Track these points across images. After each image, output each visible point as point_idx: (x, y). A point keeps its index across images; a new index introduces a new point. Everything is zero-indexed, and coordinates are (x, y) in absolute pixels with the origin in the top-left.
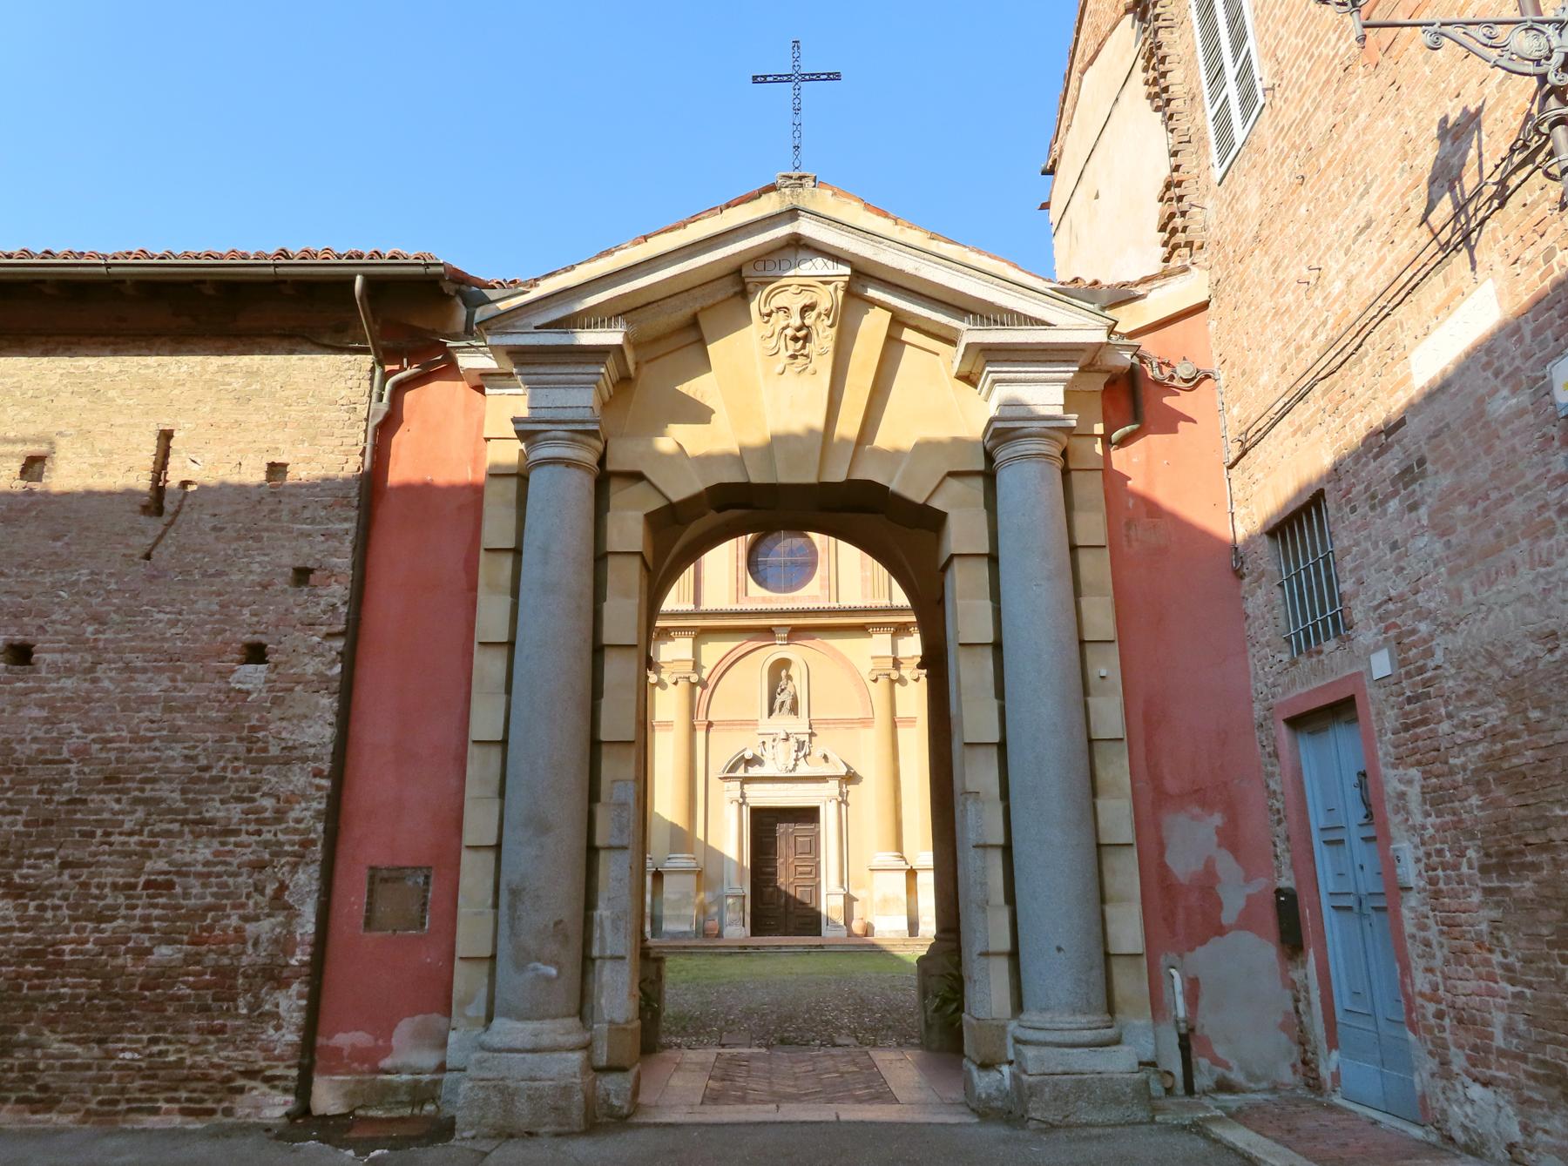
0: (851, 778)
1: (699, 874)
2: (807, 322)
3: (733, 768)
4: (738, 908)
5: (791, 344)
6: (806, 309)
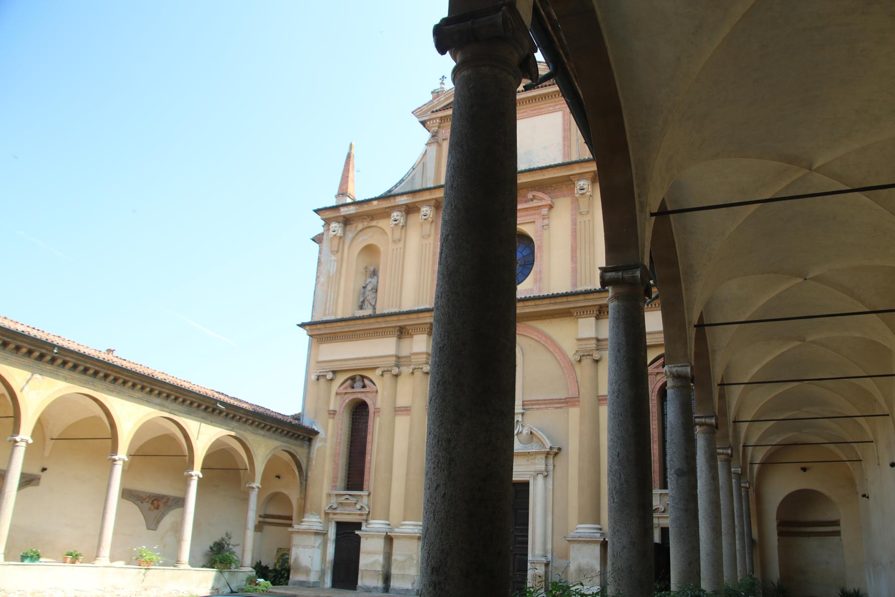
0: (554, 453)
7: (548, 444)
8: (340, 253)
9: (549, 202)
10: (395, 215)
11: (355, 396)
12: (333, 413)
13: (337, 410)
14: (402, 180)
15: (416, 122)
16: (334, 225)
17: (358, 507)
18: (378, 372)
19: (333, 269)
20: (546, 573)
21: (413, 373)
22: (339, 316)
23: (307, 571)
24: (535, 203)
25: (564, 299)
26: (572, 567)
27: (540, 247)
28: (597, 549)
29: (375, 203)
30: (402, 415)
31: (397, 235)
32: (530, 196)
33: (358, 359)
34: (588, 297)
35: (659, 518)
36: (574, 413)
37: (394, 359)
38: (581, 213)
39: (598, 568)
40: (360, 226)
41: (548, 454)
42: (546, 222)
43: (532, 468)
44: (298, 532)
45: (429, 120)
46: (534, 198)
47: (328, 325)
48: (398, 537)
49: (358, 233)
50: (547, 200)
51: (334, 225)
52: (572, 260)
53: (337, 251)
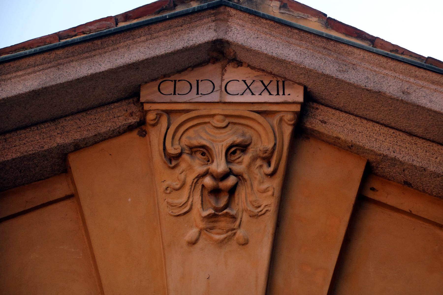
2: (237, 168)
5: (212, 200)
6: (235, 150)
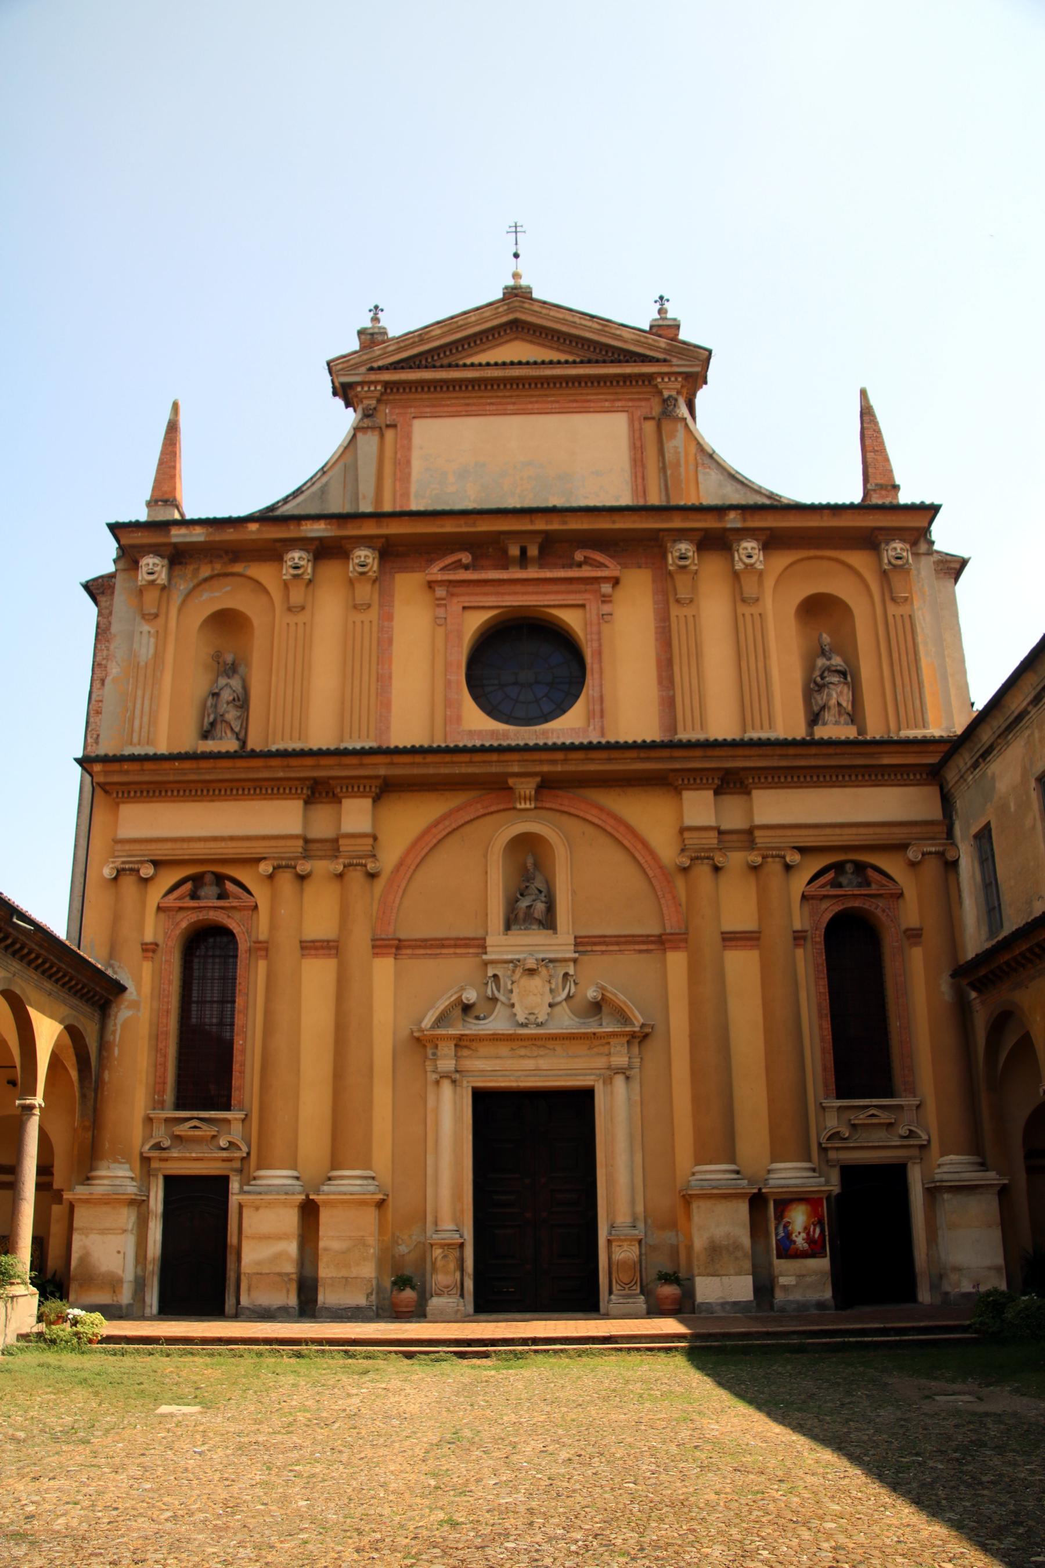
1: (381, 1204)
3: (442, 1020)
4: (452, 1266)
7: (638, 1019)
8: (161, 620)
9: (616, 573)
10: (296, 556)
11: (202, 916)
12: (150, 949)
13: (160, 941)
14: (298, 492)
15: (326, 383)
16: (149, 562)
17: (223, 1143)
18: (265, 868)
19: (146, 650)
20: (641, 1254)
21: (340, 876)
22: (163, 749)
23: (114, 1283)
24: (586, 572)
25: (665, 753)
26: (699, 1243)
27: (599, 653)
28: (743, 1208)
29: (253, 527)
30: (316, 956)
31: (297, 596)
32: (579, 556)
33: (215, 839)
34: (710, 752)
35: (838, 1149)
36: (677, 961)
37: (301, 843)
38: (678, 601)
39: (746, 1241)
40: (205, 572)
41: (633, 1035)
42: (606, 608)
43: (600, 1062)
44: (87, 1201)
45: (362, 384)
46: (587, 561)
47: (148, 766)
48: (329, 1203)
49: (199, 585)
50: (612, 569)
51: (149, 562)
52: (660, 682)
53: (156, 616)
